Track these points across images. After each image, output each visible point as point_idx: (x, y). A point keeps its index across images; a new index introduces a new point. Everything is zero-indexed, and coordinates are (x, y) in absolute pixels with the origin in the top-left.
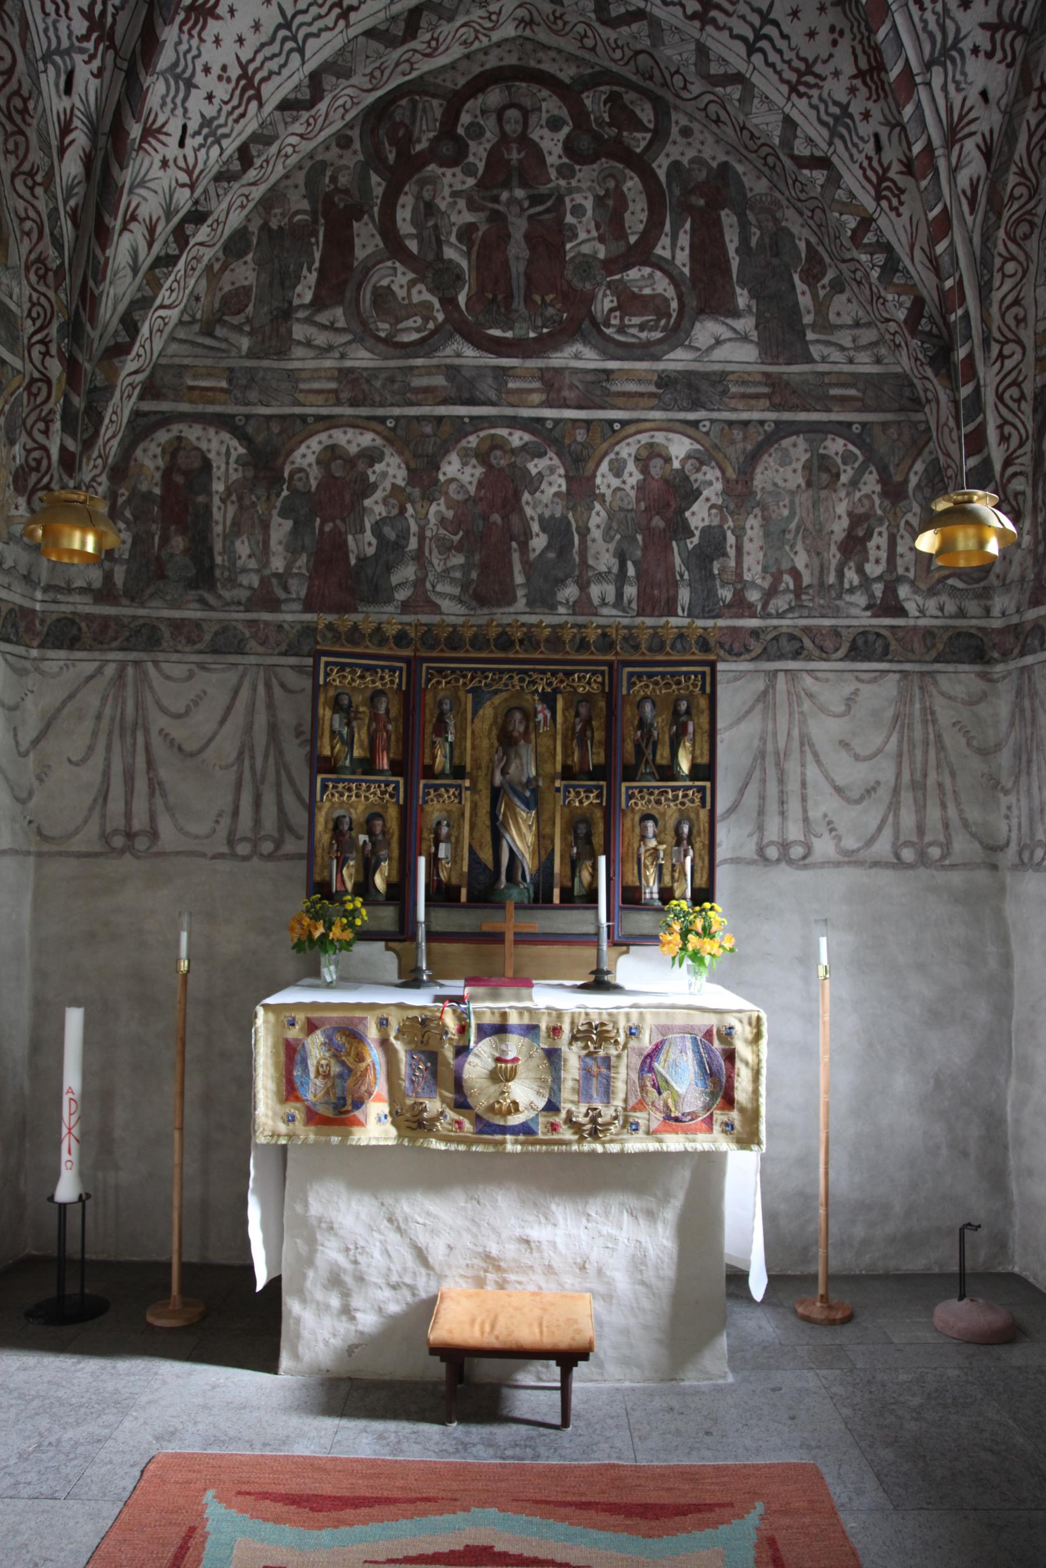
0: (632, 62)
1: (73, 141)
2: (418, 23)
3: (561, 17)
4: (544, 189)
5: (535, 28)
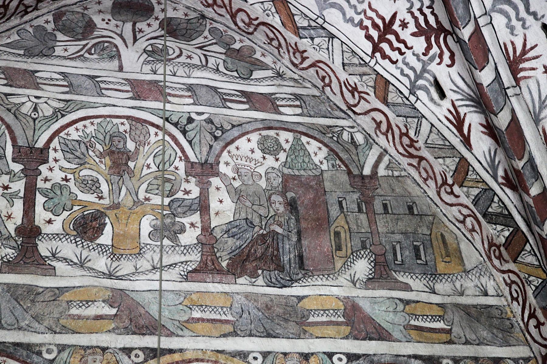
1: (470, 125)
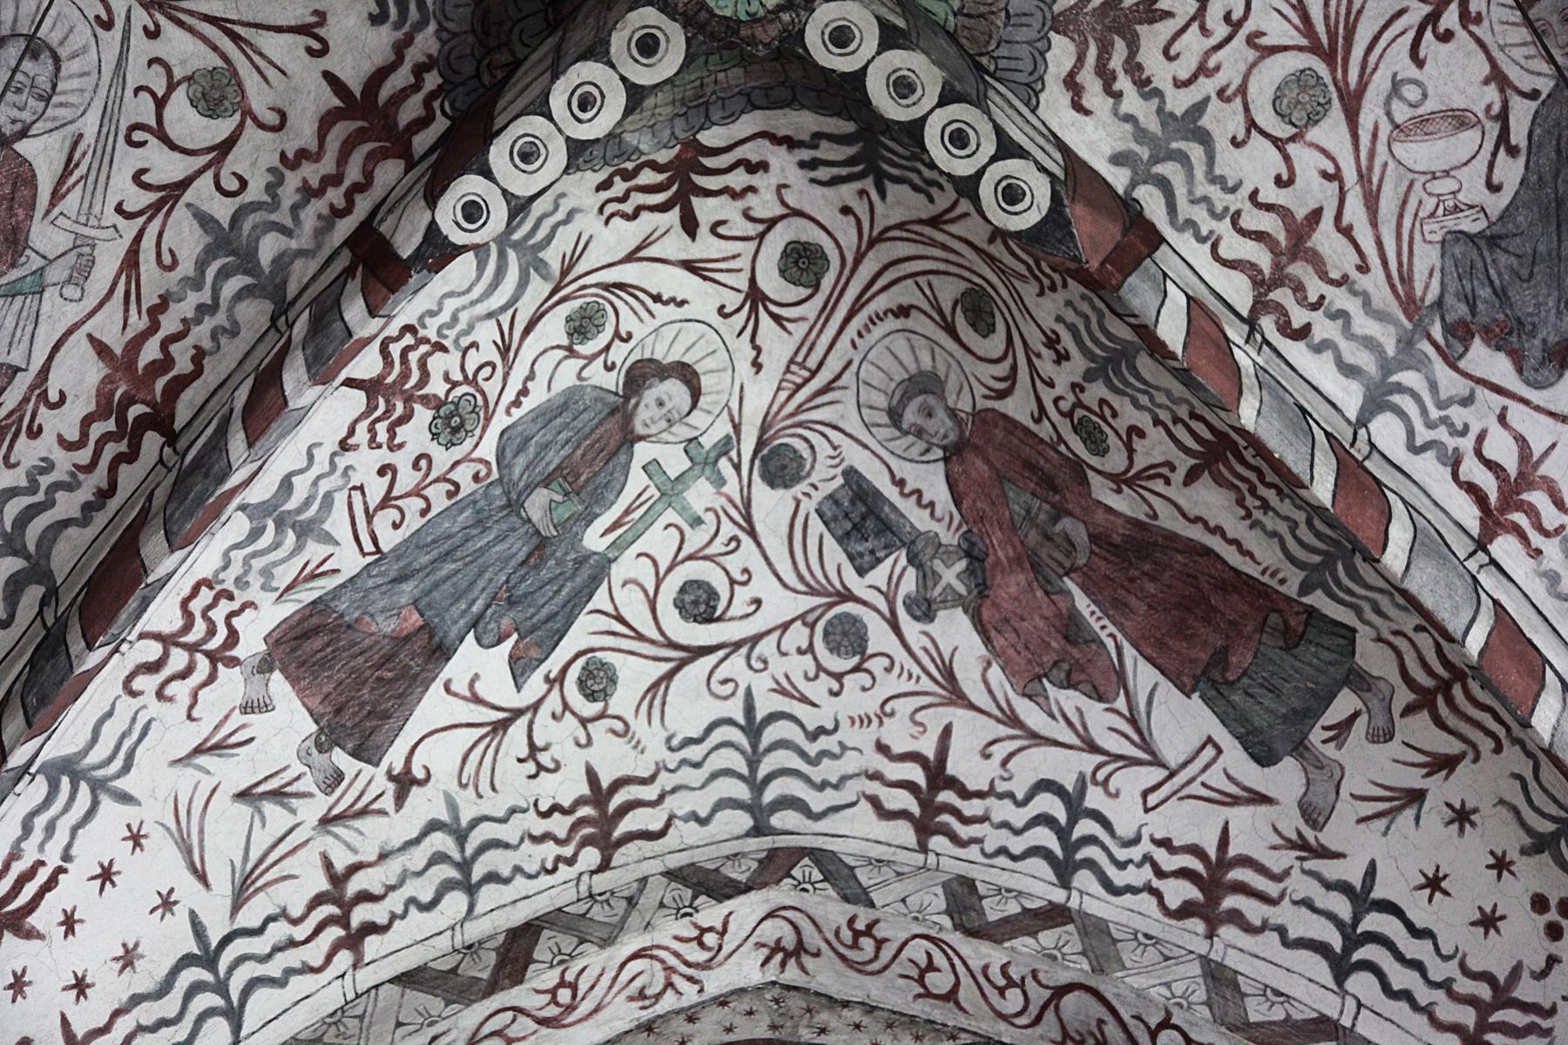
0: (1050, 1015)
2: (530, 952)
3: (868, 931)
5: (808, 961)
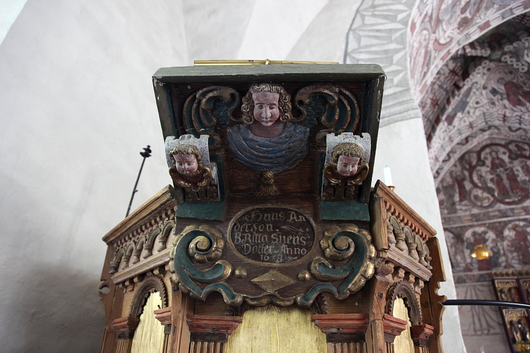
4: (507, 167)
